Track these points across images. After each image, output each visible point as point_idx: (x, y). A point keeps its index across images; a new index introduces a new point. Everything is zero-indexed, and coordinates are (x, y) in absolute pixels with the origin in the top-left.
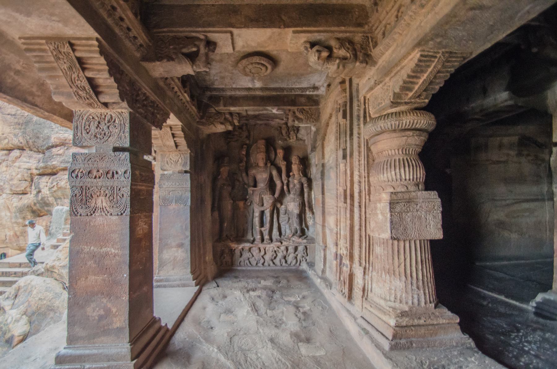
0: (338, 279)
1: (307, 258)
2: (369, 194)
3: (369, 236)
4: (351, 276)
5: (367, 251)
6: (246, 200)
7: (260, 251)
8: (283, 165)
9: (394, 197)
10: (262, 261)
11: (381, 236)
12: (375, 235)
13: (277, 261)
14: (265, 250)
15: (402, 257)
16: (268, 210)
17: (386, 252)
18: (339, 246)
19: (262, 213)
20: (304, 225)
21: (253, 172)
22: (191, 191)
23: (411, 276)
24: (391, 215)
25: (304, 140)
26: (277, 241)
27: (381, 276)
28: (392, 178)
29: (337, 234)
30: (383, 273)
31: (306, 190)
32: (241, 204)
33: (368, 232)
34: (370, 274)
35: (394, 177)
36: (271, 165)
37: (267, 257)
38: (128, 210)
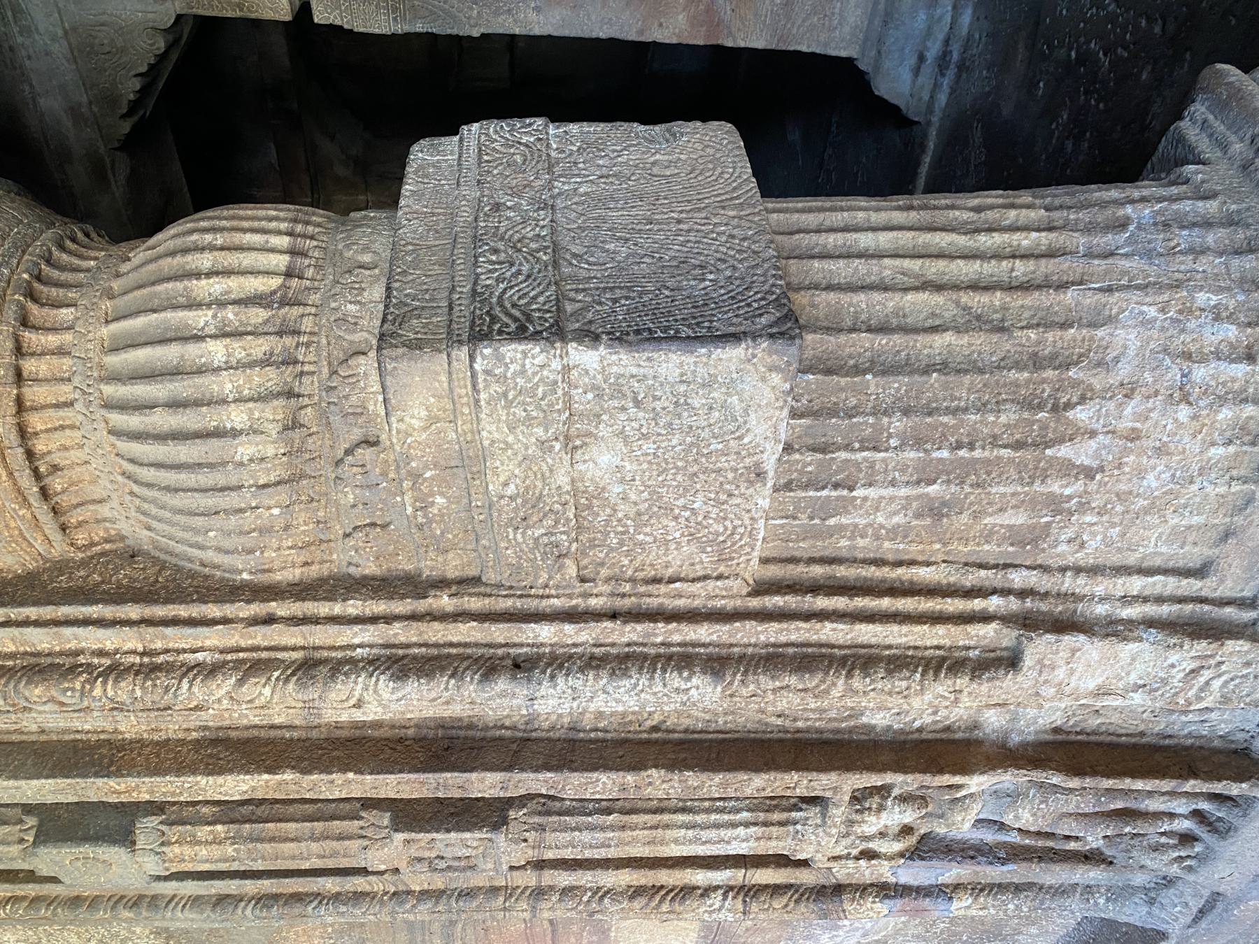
0: (1094, 874)
2: (415, 585)
3: (762, 588)
4: (1074, 753)
5: (885, 603)
11: (770, 464)
12: (757, 526)
17: (897, 424)
18: (843, 872)
23: (1051, 254)
24: (590, 336)
27: (1089, 473)
28: (266, 362)
29: (749, 892)
30: (1064, 451)
33: (729, 594)
34: (1068, 583)
35: (259, 347)
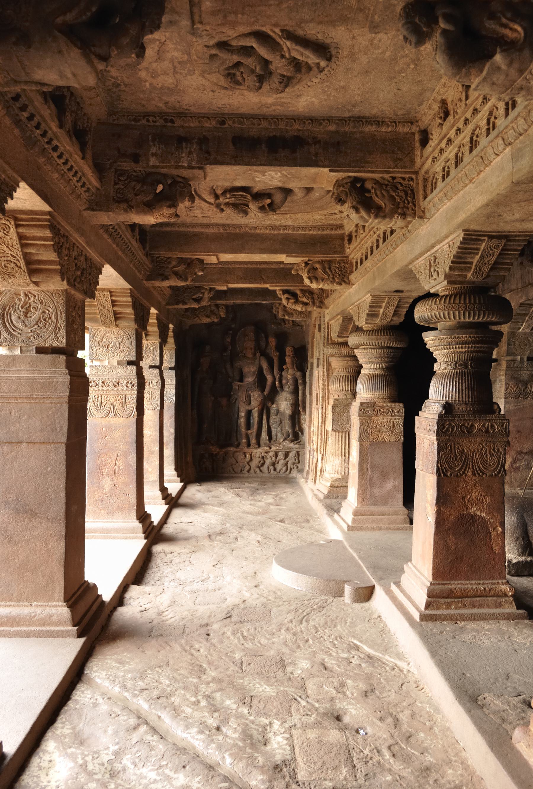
1: (299, 465)
6: (230, 396)
7: (245, 456)
8: (275, 355)
9: (336, 402)
10: (247, 467)
13: (265, 468)
14: (251, 455)
15: (340, 443)
16: (256, 409)
19: (249, 413)
20: (297, 429)
21: (239, 364)
22: (176, 388)
25: (302, 326)
26: (266, 445)
31: (300, 387)
32: (224, 401)
36: (261, 355)
37: (253, 464)
38: (159, 407)
